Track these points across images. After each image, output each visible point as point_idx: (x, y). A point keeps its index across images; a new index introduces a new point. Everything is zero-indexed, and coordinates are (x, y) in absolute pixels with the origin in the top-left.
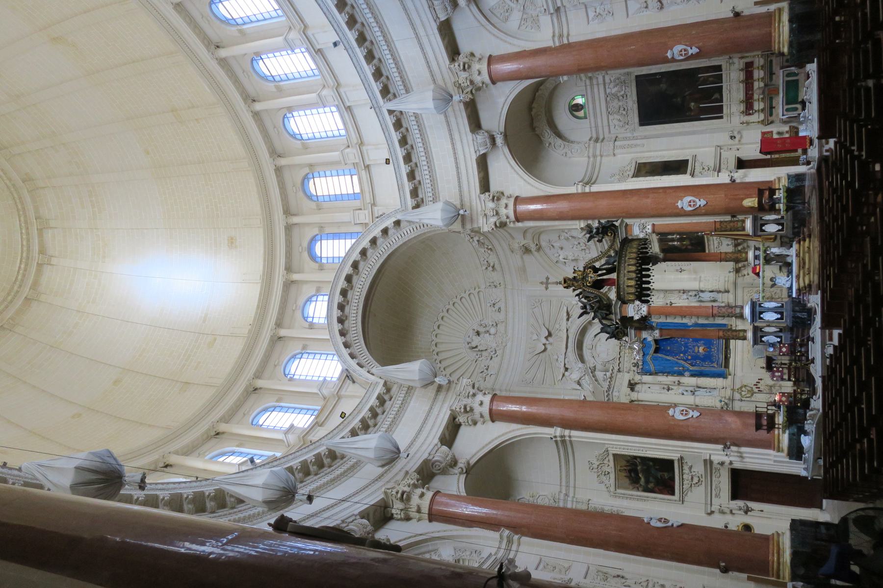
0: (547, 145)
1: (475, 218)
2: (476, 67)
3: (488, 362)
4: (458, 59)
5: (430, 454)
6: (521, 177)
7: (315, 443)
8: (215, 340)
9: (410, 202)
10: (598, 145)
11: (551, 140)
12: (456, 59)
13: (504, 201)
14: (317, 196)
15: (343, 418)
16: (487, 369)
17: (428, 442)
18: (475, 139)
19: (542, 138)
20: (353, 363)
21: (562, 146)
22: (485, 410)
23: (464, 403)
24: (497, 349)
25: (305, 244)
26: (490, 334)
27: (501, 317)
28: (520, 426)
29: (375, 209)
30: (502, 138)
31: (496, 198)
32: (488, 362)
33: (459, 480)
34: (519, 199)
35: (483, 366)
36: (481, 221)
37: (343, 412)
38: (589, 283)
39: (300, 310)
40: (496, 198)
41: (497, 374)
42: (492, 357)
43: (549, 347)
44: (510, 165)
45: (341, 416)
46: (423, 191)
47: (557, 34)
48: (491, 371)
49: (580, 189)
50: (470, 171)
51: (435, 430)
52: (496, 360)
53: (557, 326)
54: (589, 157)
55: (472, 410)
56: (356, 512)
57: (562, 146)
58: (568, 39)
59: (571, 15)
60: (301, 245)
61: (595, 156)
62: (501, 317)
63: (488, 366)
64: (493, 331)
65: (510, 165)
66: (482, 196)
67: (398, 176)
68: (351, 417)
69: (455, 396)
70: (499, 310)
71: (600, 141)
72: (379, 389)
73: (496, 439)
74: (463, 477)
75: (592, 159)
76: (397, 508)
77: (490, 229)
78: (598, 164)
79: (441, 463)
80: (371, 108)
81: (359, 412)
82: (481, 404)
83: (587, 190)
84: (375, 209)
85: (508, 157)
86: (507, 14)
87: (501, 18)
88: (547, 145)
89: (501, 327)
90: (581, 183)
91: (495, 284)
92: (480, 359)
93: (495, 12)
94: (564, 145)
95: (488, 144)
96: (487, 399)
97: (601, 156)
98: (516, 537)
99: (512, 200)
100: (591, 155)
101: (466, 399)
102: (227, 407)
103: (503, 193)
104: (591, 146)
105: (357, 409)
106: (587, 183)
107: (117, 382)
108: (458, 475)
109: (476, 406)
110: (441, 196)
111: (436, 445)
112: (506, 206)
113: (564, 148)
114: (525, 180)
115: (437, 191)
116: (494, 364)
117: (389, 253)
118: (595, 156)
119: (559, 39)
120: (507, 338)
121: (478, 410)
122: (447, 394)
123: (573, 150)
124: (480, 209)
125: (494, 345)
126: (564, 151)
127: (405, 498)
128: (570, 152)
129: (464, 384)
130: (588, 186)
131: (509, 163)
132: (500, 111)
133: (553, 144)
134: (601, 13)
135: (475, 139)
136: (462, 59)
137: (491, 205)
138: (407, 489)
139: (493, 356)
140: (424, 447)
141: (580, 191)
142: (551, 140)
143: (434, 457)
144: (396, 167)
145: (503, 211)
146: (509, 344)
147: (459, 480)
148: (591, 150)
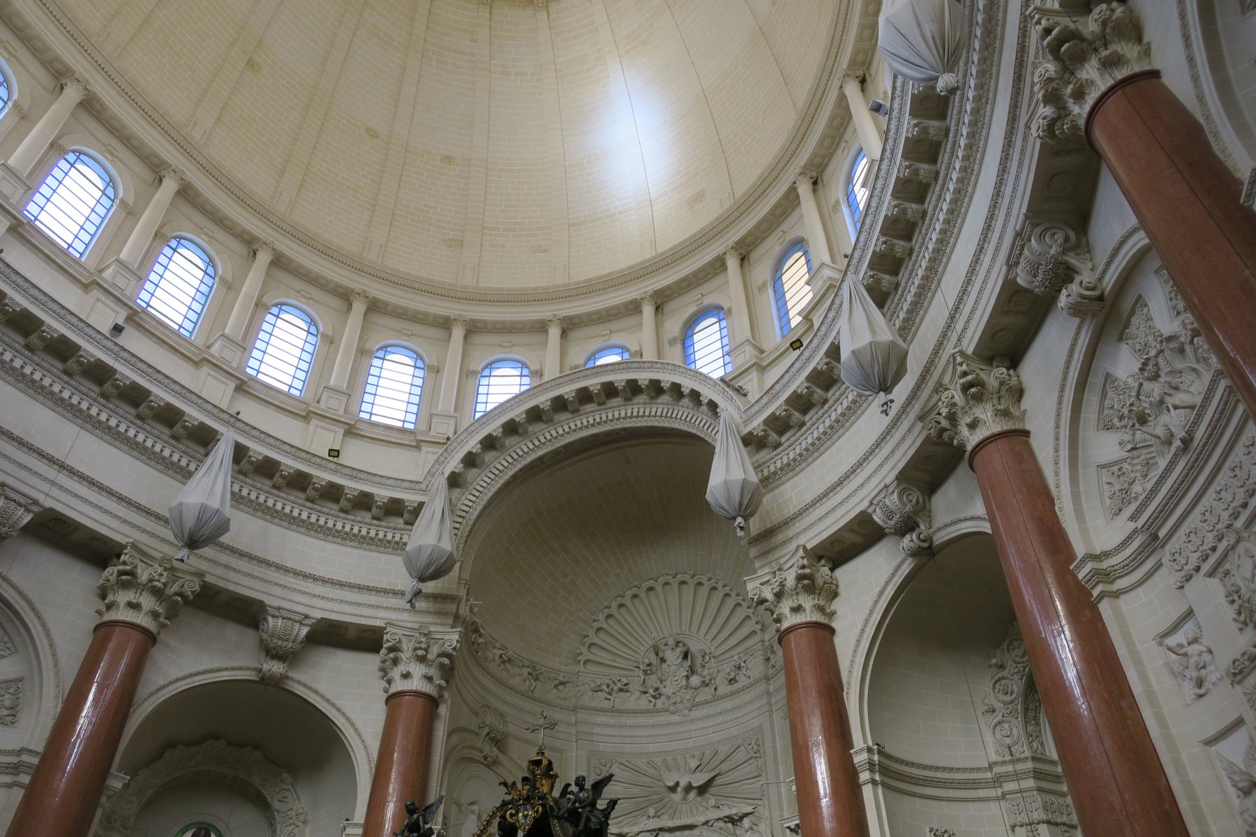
0: (994, 661)
1: (771, 557)
2: (985, 412)
3: (635, 686)
4: (998, 367)
5: (279, 609)
6: (867, 621)
7: (240, 420)
8: (545, 251)
9: (756, 425)
10: (1030, 783)
11: (1011, 668)
12: (995, 365)
13: (807, 602)
14: (781, 277)
15: (329, 456)
16: (621, 690)
17: (315, 602)
18: (891, 489)
19: (1005, 644)
20: (472, 444)
21: (1008, 698)
22: (399, 685)
23: (405, 647)
24: (663, 698)
25: (708, 301)
26: (687, 677)
27: (724, 688)
28: (375, 755)
29: (754, 375)
30: (912, 544)
31: (807, 583)
32: (635, 686)
33: (248, 669)
34: (826, 633)
35: (624, 680)
36: (766, 570)
37: (338, 451)
38: (512, 815)
39: (604, 344)
40: (807, 583)
41: (612, 711)
42: (645, 693)
43: (677, 797)
44: (885, 588)
45: (330, 450)
46: (793, 439)
47: (1105, 564)
48: (619, 700)
49: (860, 759)
50: (843, 510)
51: (347, 609)
52: (644, 703)
53: (712, 801)
54: (991, 767)
55: (395, 662)
56: (49, 503)
57: (1008, 698)
58: (1102, 595)
59: (1166, 579)
60: (703, 295)
61: (998, 781)
62: (724, 688)
63: (627, 691)
64: (695, 680)
65: (885, 588)
66: (801, 552)
67: (787, 377)
68: (333, 466)
69: (416, 626)
70: (732, 681)
71: (1044, 785)
72: (411, 498)
73: (348, 719)
74: (251, 676)
75: (989, 775)
76: (112, 571)
77: (750, 595)
78: (981, 793)
79: (267, 633)
80: (846, 256)
81: (351, 477)
82: (406, 676)
83: (864, 776)
84: (754, 375)
85: (896, 578)
86: (1116, 421)
87: (1106, 412)
88: (994, 661)
89: (705, 694)
90: (876, 758)
91: (772, 657)
92: (641, 674)
93: (1111, 394)
94: (1012, 702)
95: (893, 523)
96: (416, 684)
97: (1004, 796)
98: (25, 779)
99: (817, 617)
100: (997, 770)
101: (411, 646)
102: (403, 303)
103: (835, 595)
104: (1020, 766)
105: (356, 473)
106: (884, 771)
107: (448, 160)
108: (255, 665)
109: (402, 668)
110: (799, 476)
111: (307, 617)
112: (797, 609)
113: (1005, 703)
114: (863, 631)
115: (804, 464)
116: (635, 700)
117: (699, 433)
118: (998, 781)
119: (1096, 572)
120: (686, 712)
121: (396, 673)
122: (431, 613)
123: (1006, 726)
124: (782, 561)
125: (668, 691)
126: (997, 705)
127: (128, 580)
128: (999, 718)
129: (447, 637)
130: (877, 777)
131: (887, 583)
132: (961, 516)
133: (1005, 673)
134: (1192, 661)
135: (891, 489)
136: (994, 376)
137: (790, 578)
138: (143, 575)
139: (647, 695)
140: (315, 602)
141: (856, 760)
142: (1011, 668)
143: (273, 616)
144: (797, 365)
145: (785, 607)
146: (675, 718)
147: (248, 669)
148: (1010, 768)
